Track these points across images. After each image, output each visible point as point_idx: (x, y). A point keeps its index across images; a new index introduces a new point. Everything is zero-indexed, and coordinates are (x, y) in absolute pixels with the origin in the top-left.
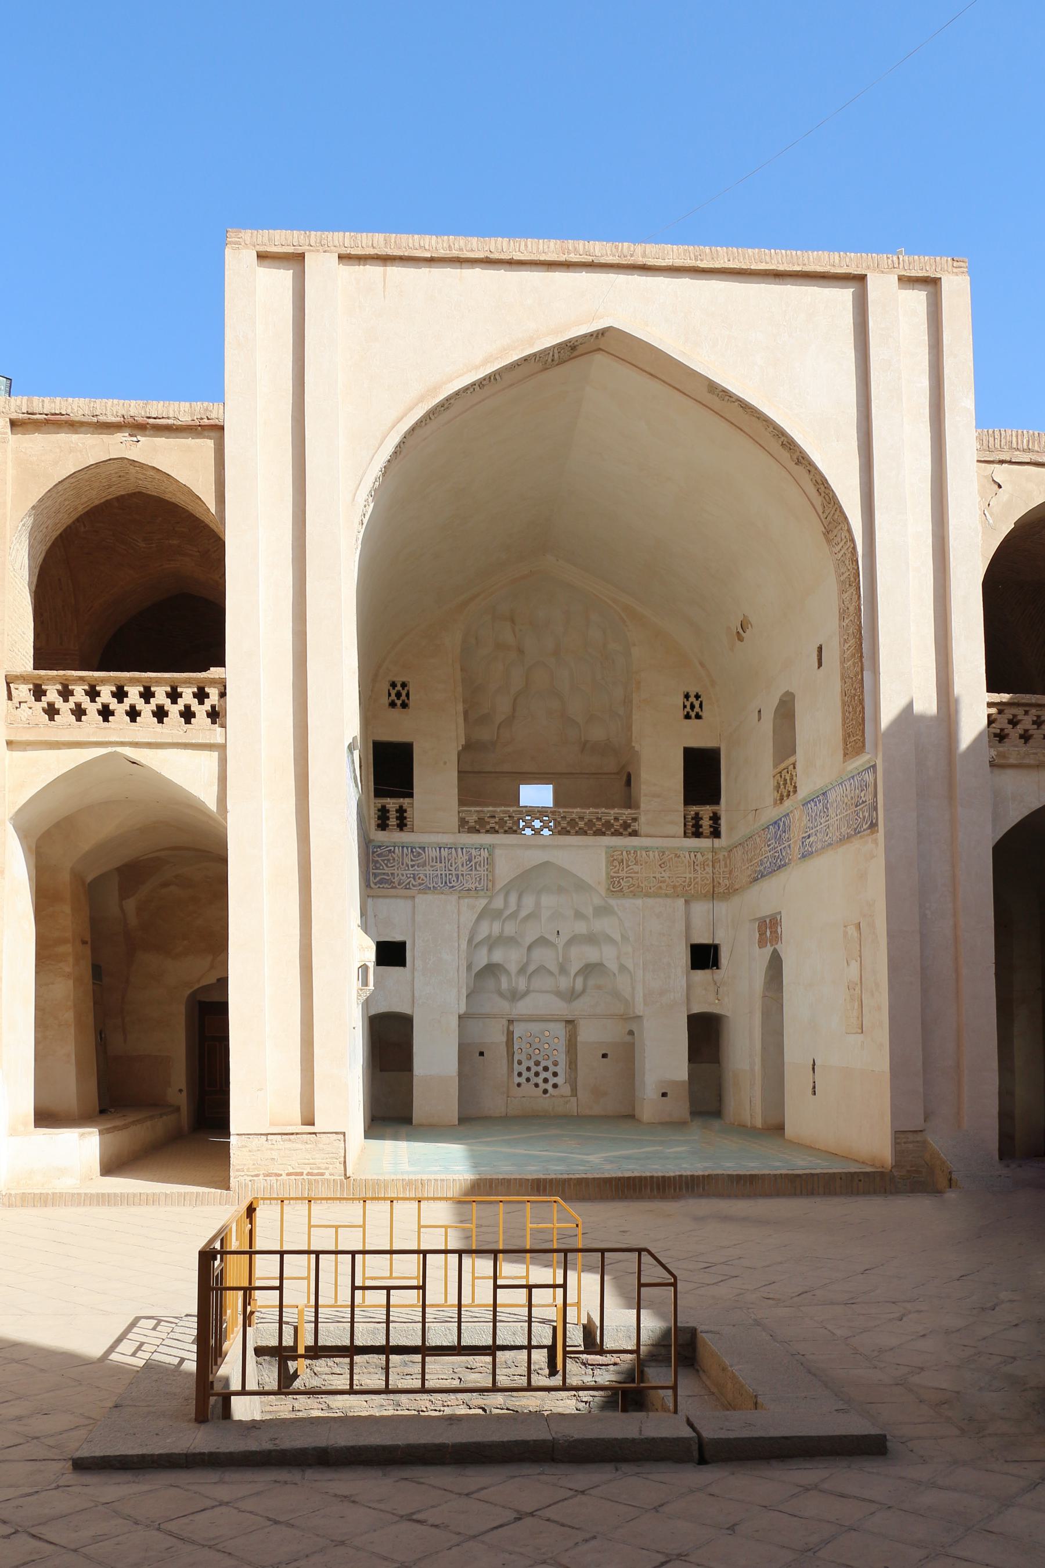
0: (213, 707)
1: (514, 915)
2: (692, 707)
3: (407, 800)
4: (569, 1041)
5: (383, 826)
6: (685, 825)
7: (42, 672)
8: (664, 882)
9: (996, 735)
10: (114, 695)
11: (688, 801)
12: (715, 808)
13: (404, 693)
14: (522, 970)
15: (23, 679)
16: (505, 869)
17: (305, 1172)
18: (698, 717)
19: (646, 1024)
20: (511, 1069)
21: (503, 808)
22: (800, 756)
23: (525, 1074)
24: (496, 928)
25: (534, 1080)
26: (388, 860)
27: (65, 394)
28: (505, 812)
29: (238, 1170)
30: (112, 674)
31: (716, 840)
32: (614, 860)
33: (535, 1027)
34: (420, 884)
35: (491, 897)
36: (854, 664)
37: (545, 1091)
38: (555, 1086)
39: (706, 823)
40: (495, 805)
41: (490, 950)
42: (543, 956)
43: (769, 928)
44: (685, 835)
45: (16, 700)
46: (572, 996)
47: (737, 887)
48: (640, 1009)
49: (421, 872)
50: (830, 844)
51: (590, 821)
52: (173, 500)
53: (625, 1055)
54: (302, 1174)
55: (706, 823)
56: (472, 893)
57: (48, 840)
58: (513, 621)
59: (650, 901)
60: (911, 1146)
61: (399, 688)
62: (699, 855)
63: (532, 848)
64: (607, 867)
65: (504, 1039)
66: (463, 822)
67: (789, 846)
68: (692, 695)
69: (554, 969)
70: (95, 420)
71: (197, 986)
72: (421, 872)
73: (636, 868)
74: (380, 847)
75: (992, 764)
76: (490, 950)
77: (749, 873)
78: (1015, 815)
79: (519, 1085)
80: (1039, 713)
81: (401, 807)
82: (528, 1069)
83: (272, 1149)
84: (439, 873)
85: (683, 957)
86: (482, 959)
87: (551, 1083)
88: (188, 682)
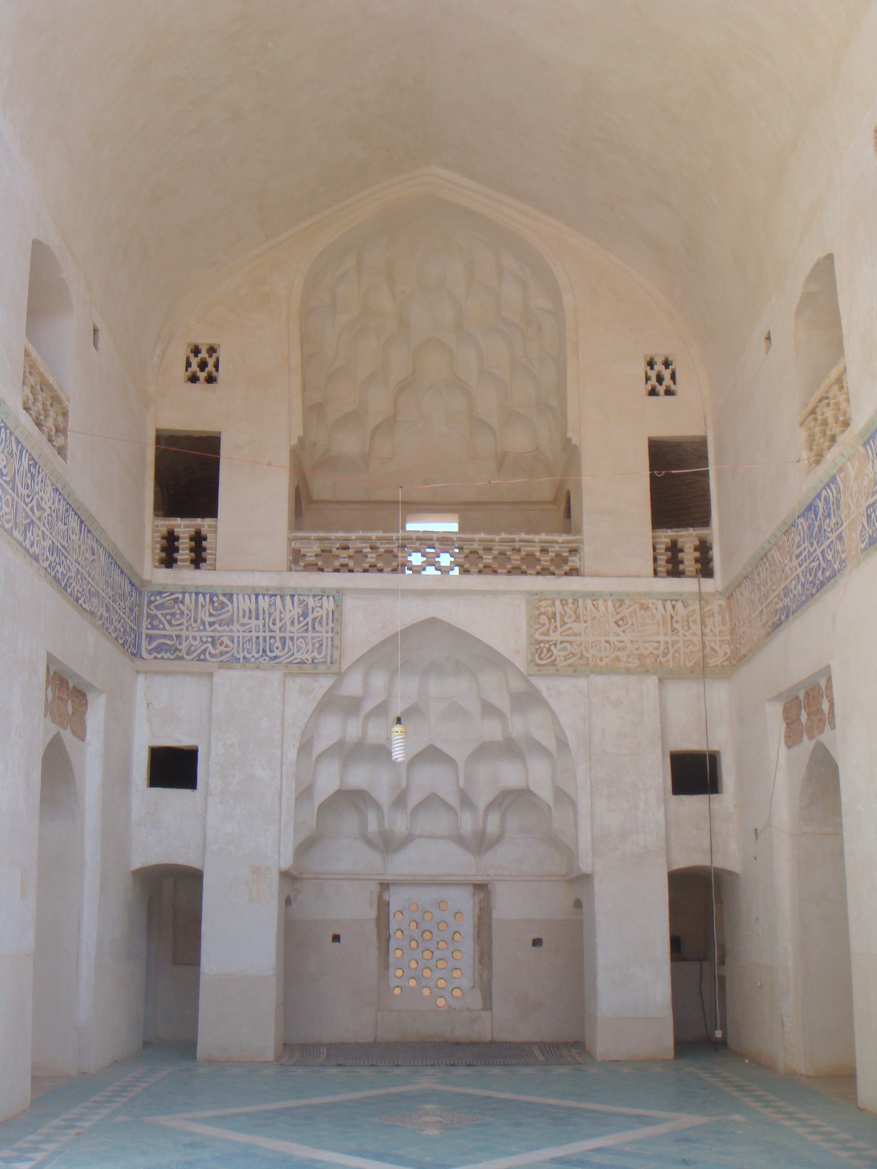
1: (381, 709)
4: (480, 918)
5: (169, 560)
6: (655, 560)
8: (624, 649)
13: (211, 362)
14: (400, 801)
19: (599, 886)
21: (361, 534)
24: (353, 730)
26: (173, 615)
28: (361, 539)
32: (540, 611)
33: (426, 896)
34: (222, 654)
35: (340, 676)
39: (689, 557)
40: (347, 529)
46: (480, 844)
47: (743, 652)
51: (502, 553)
53: (568, 942)
55: (689, 557)
56: (308, 667)
59: (600, 681)
62: (679, 605)
64: (529, 626)
65: (373, 914)
66: (297, 558)
67: (840, 537)
69: (452, 799)
73: (578, 627)
74: (160, 593)
77: (765, 618)
84: (254, 634)
86: (328, 780)
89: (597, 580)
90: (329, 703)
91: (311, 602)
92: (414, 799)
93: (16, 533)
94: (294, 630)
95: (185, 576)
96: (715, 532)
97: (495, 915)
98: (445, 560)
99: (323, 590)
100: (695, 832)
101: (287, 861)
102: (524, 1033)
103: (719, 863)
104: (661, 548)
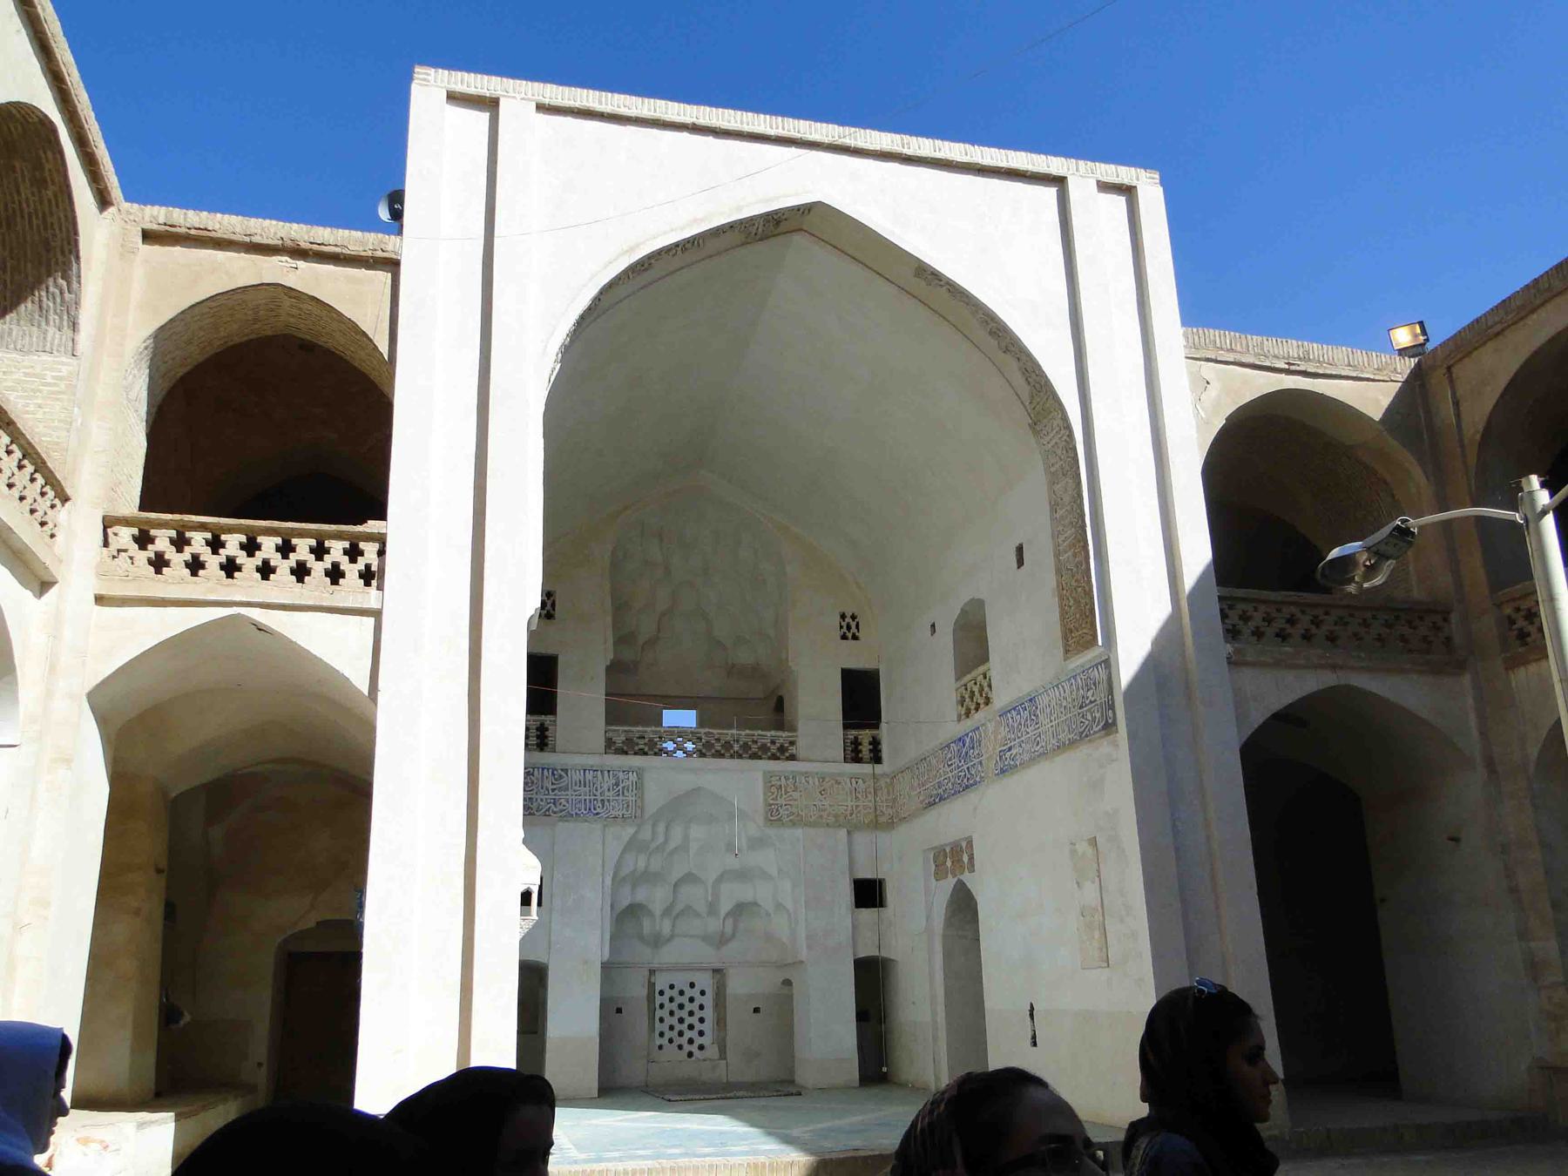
0: (368, 567)
2: (849, 628)
3: (550, 717)
7: (153, 515)
10: (242, 547)
12: (875, 732)
14: (667, 912)
15: (126, 522)
16: (655, 797)
18: (855, 637)
20: (652, 1028)
22: (995, 666)
23: (668, 1034)
25: (678, 1041)
27: (212, 209)
28: (655, 732)
30: (242, 521)
35: (639, 826)
36: (1075, 555)
37: (690, 1054)
38: (701, 1047)
39: (865, 749)
41: (634, 887)
42: (690, 894)
43: (954, 858)
44: (845, 761)
45: (114, 546)
46: (721, 940)
48: (804, 954)
51: (746, 744)
52: (329, 345)
53: (780, 1008)
55: (865, 749)
57: (135, 722)
59: (811, 831)
63: (670, 775)
65: (645, 992)
66: (610, 745)
68: (848, 615)
70: (247, 239)
71: (290, 933)
73: (796, 795)
75: (1230, 661)
76: (634, 887)
78: (1257, 717)
79: (660, 1047)
85: (847, 894)
88: (339, 536)
90: (632, 845)
96: (884, 732)
97: (729, 991)
102: (749, 1076)
103: (884, 954)
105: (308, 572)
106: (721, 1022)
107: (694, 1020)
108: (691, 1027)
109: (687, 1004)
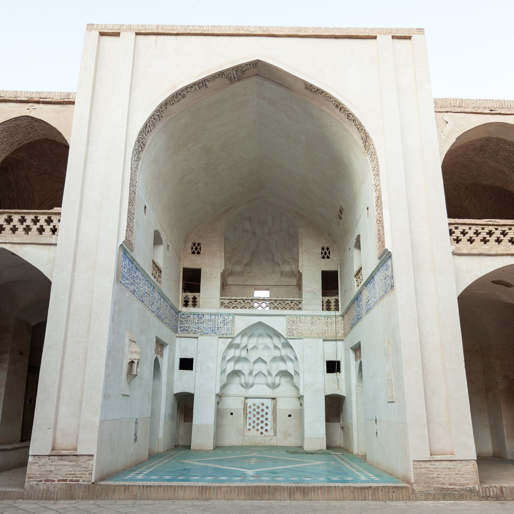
1: (246, 347)
2: (325, 253)
3: (197, 294)
4: (273, 408)
5: (186, 304)
6: (323, 305)
8: (313, 331)
9: (454, 240)
11: (324, 295)
13: (199, 248)
14: (251, 373)
17: (69, 479)
18: (328, 257)
23: (252, 424)
25: (257, 427)
29: (30, 478)
31: (337, 312)
33: (258, 402)
34: (201, 332)
37: (262, 433)
38: (266, 430)
39: (333, 305)
49: (201, 326)
50: (377, 302)
54: (66, 480)
55: (333, 305)
58: (250, 221)
60: (423, 470)
61: (197, 246)
62: (329, 319)
64: (287, 324)
65: (243, 407)
66: (222, 304)
68: (325, 248)
72: (201, 326)
73: (300, 325)
79: (249, 430)
80: (477, 229)
81: (194, 297)
82: (254, 422)
83: (52, 465)
86: (230, 367)
87: (264, 429)
89: (306, 311)
90: (230, 346)
91: (226, 317)
92: (254, 373)
93: (150, 307)
94: (221, 325)
95: (190, 309)
98: (264, 305)
99: (230, 314)
100: (334, 385)
101: (218, 391)
104: (325, 302)
105: (43, 230)
106: (275, 420)
107: (263, 419)
108: (262, 422)
109: (260, 412)
